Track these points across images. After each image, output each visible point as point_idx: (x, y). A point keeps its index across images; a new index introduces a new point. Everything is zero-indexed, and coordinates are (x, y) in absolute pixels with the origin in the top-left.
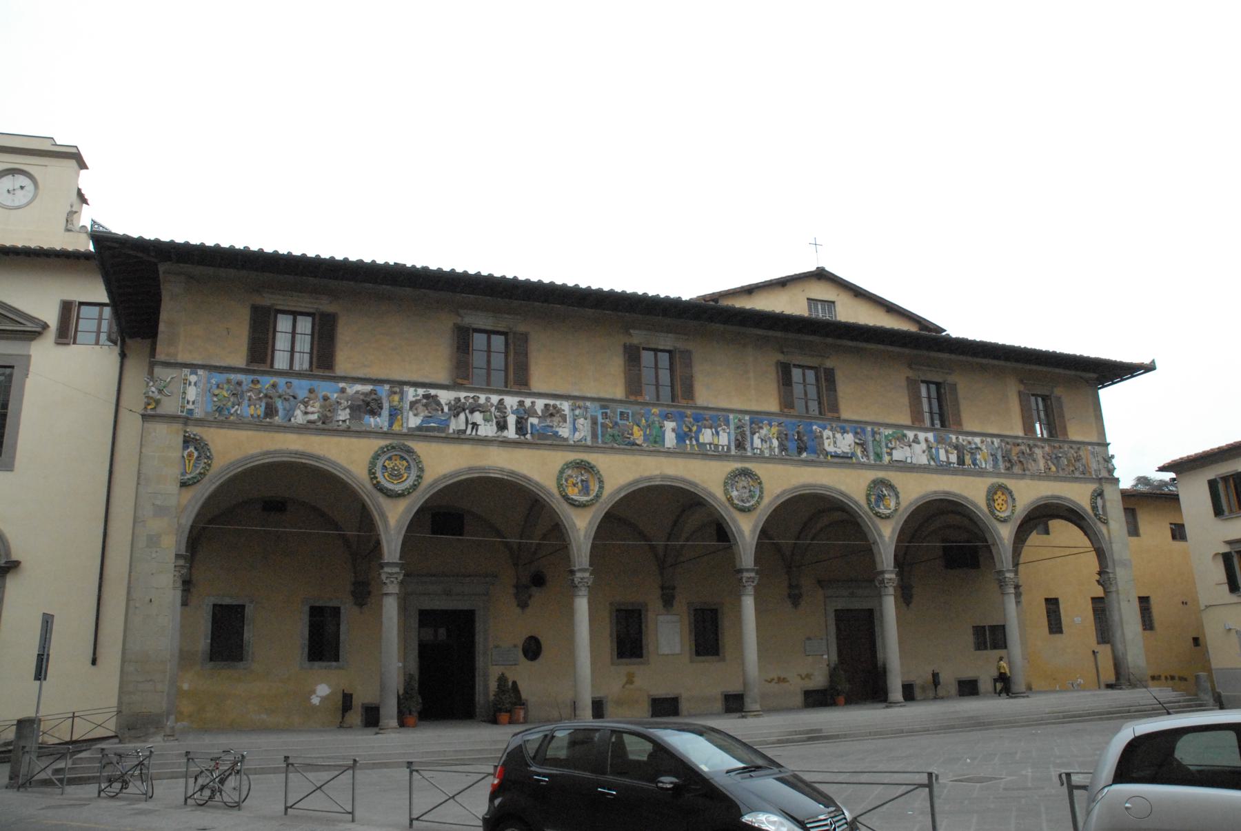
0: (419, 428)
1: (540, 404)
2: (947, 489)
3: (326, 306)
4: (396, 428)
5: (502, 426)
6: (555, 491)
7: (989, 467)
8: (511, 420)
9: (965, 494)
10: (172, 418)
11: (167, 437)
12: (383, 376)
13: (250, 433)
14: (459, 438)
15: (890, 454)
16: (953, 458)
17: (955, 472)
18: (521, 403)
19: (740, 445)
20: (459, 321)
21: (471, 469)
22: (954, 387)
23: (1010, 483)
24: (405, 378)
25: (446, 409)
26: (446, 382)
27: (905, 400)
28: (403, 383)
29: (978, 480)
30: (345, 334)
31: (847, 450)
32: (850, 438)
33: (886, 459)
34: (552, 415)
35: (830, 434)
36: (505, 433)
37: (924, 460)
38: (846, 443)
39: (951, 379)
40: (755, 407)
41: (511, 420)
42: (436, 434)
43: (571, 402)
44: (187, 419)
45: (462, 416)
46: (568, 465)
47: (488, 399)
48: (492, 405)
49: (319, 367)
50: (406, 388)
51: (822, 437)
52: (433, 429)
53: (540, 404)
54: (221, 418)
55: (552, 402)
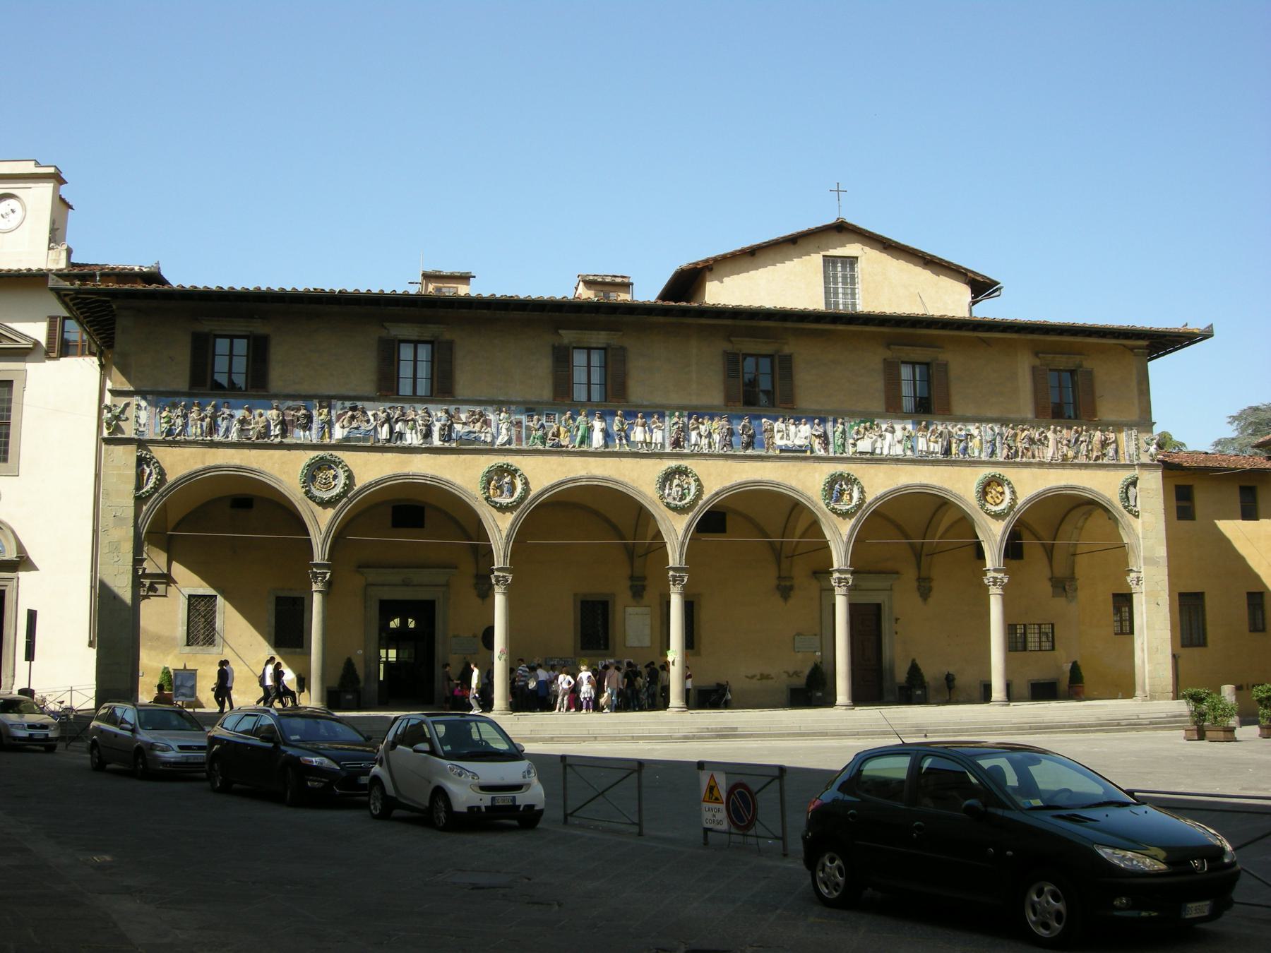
0: (347, 439)
2: (925, 482)
3: (259, 328)
4: (327, 441)
5: (427, 435)
7: (984, 457)
9: (946, 486)
10: (128, 441)
11: (125, 457)
12: (312, 393)
15: (854, 445)
16: (937, 447)
17: (935, 462)
19: (676, 443)
20: (384, 333)
21: (396, 477)
22: (945, 366)
23: (1008, 473)
24: (332, 393)
26: (373, 395)
27: (878, 384)
29: (966, 471)
30: (277, 353)
31: (798, 442)
32: (805, 429)
33: (850, 450)
35: (783, 426)
37: (898, 450)
38: (800, 434)
39: (944, 356)
40: (695, 401)
42: (361, 444)
44: (141, 443)
49: (252, 387)
50: (334, 402)
51: (772, 430)
52: (359, 440)
54: (171, 439)
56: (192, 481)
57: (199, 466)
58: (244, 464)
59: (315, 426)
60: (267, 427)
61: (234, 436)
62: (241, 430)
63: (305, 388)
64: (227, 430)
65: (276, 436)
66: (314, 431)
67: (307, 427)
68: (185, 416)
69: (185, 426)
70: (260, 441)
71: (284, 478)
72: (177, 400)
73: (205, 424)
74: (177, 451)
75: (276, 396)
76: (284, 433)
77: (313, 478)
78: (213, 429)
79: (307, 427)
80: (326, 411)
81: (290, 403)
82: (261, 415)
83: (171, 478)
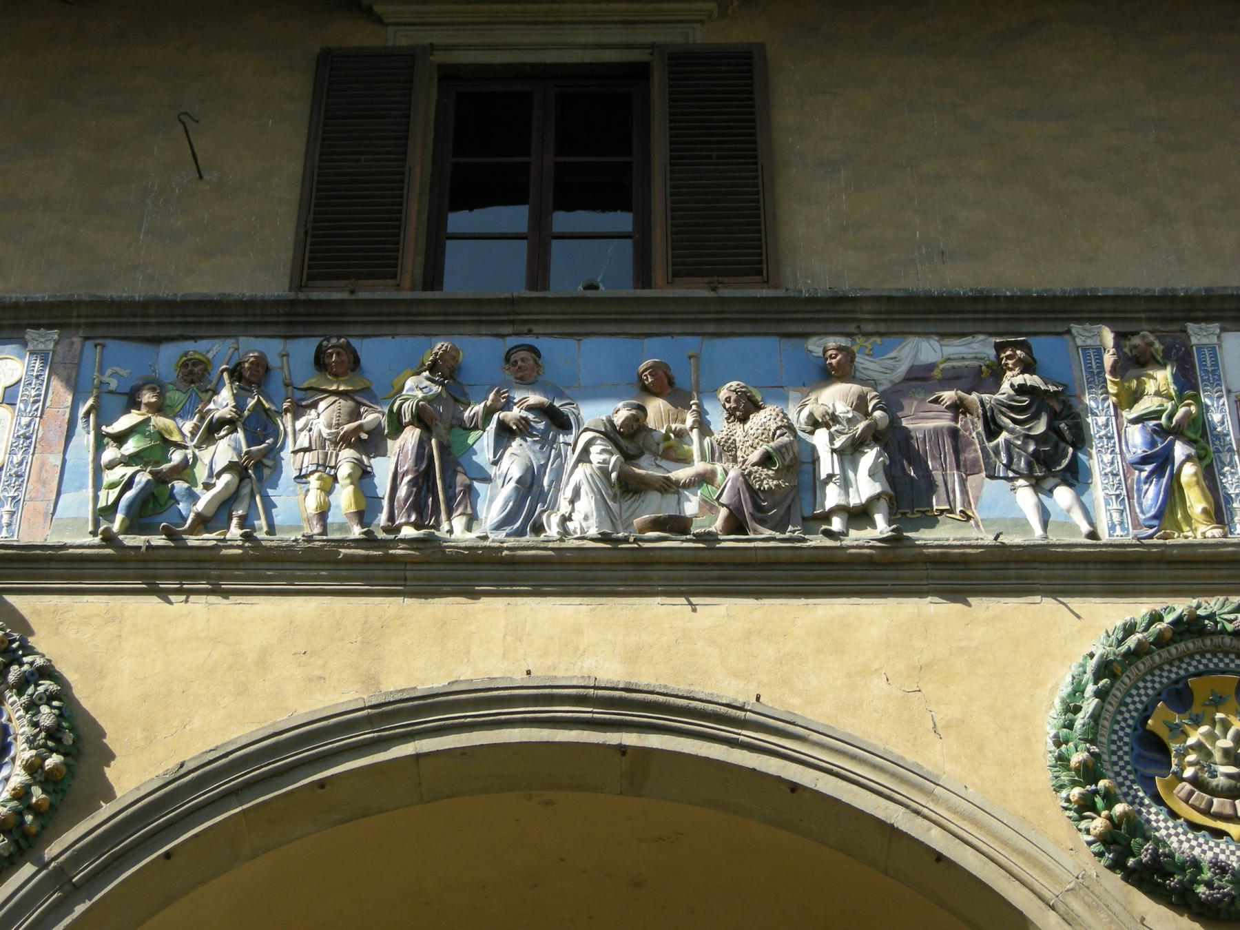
13: (313, 603)
50: (1200, 335)
56: (273, 789)
57: (340, 694)
58: (652, 676)
59: (1098, 461)
60: (792, 462)
61: (578, 513)
62: (627, 487)
63: (1010, 274)
64: (531, 488)
65: (860, 515)
66: (1099, 489)
67: (1057, 456)
68: (260, 426)
69: (255, 472)
70: (762, 537)
71: (934, 757)
72: (218, 351)
73: (382, 469)
74: (198, 614)
75: (836, 311)
76: (909, 493)
77: (1153, 751)
78: (441, 480)
79: (1057, 456)
80: (1162, 378)
81: (928, 351)
82: (744, 409)
83: (132, 776)
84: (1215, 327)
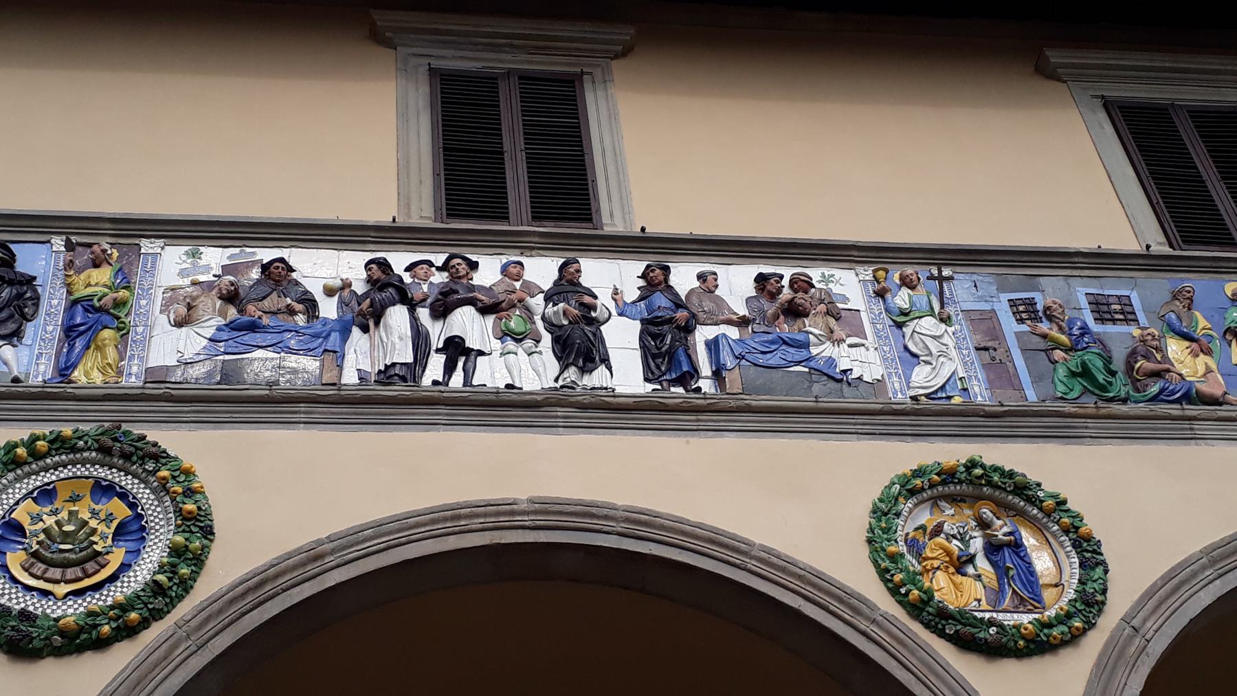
1: (737, 283)
6: (863, 581)
8: (622, 338)
14: (393, 399)
18: (655, 282)
25: (329, 309)
28: (134, 228)
34: (794, 312)
36: (599, 377)
41: (622, 338)
43: (867, 273)
45: (397, 316)
46: (914, 487)
47: (511, 272)
48: (530, 289)
50: (147, 246)
53: (737, 283)
55: (787, 272)
84: (160, 242)
